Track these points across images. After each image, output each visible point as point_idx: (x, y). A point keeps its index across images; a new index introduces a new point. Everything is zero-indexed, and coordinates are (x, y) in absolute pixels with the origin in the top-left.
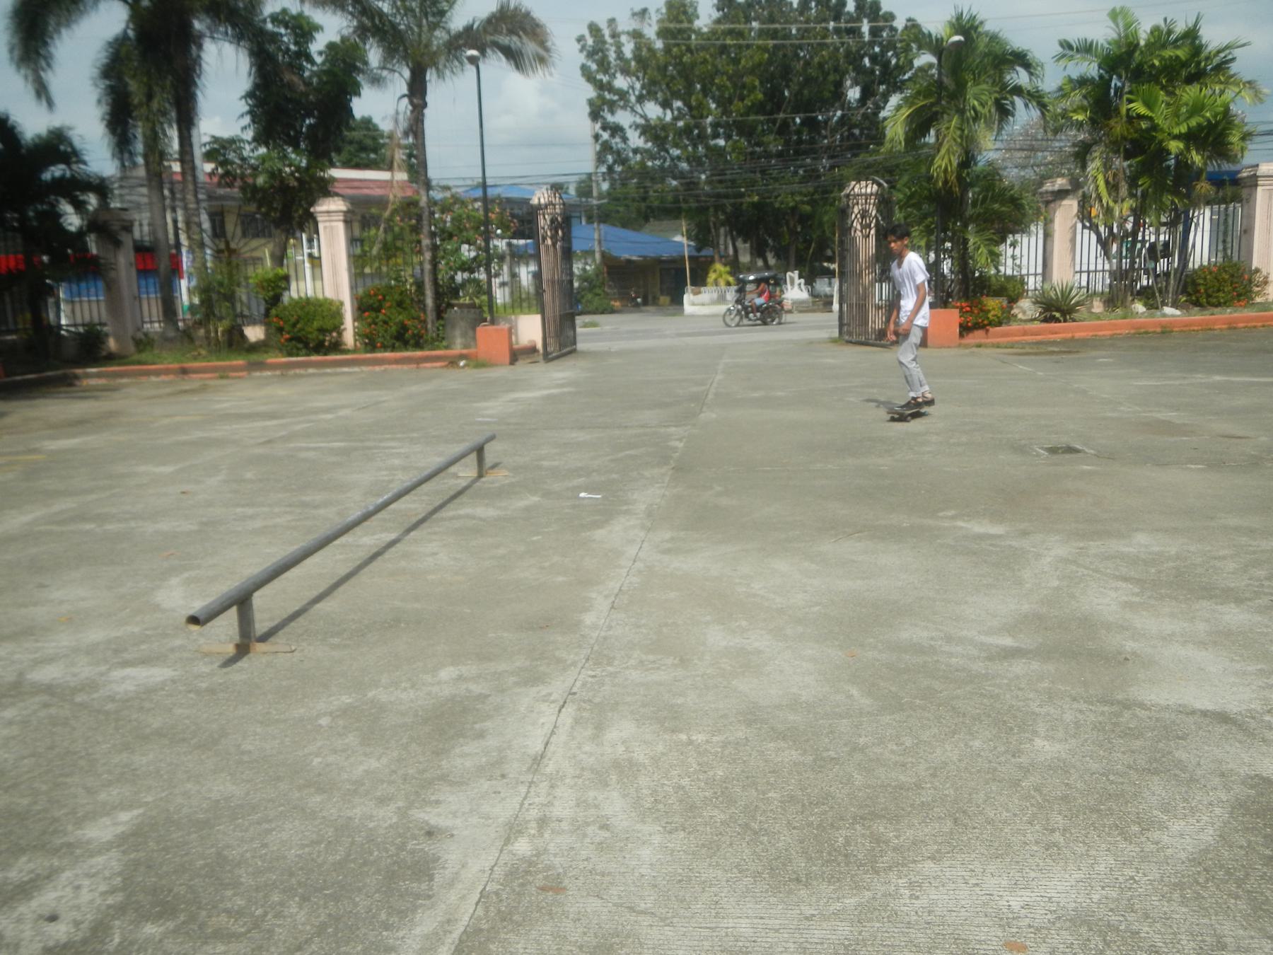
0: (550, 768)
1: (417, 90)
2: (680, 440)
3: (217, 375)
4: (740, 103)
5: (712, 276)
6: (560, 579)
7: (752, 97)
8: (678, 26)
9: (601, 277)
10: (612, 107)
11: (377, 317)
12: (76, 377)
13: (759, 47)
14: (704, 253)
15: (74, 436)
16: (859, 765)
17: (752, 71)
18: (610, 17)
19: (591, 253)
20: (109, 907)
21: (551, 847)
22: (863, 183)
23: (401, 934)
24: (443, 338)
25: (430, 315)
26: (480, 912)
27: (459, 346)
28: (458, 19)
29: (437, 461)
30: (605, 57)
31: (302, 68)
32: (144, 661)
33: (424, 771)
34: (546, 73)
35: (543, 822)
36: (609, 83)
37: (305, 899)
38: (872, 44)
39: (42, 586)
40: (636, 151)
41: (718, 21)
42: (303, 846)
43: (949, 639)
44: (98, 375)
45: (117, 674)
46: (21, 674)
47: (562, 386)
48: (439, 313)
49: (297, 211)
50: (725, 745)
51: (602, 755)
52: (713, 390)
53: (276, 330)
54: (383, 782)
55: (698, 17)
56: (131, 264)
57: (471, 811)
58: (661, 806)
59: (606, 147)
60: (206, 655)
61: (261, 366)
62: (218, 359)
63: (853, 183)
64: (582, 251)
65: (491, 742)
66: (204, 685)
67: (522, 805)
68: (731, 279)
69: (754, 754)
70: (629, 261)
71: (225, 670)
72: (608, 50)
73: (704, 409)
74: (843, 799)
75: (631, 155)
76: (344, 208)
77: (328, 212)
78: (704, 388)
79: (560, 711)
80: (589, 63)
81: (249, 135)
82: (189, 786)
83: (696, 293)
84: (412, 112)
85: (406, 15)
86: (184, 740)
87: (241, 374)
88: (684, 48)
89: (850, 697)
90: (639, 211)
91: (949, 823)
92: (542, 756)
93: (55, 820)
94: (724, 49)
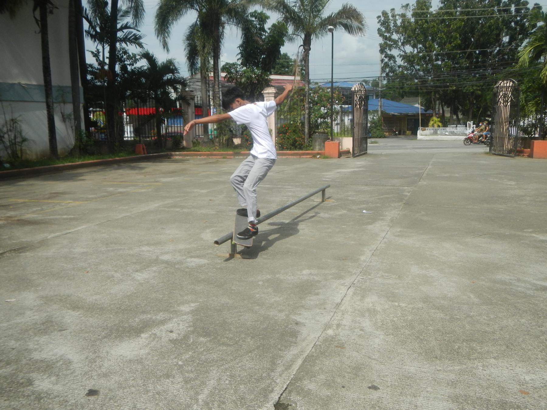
0: (343, 308)
1: (307, 43)
2: (409, 192)
3: (222, 157)
4: (450, 46)
5: (431, 123)
6: (352, 242)
7: (455, 42)
8: (422, 11)
11: (285, 136)
12: (172, 155)
13: (460, 20)
14: (429, 112)
15: (171, 177)
16: (469, 322)
17: (456, 30)
19: (376, 111)
20: (189, 331)
21: (341, 334)
22: (505, 82)
23: (285, 353)
24: (311, 146)
25: (306, 136)
26: (313, 350)
28: (326, 13)
29: (306, 194)
30: (389, 25)
31: (261, 35)
32: (198, 257)
33: (296, 303)
34: (362, 35)
35: (338, 325)
36: (390, 37)
37: (252, 337)
38: (516, 16)
39: (163, 228)
40: (399, 67)
41: (441, 8)
42: (252, 322)
43: (519, 280)
44: (179, 155)
45: (189, 260)
46: (157, 257)
47: (360, 167)
48: (310, 135)
49: (256, 92)
50: (413, 309)
51: (363, 306)
52: (426, 172)
54: (281, 305)
57: (312, 318)
58: (385, 326)
59: (386, 65)
60: (219, 257)
61: (238, 154)
62: (223, 151)
63: (501, 81)
65: (321, 297)
66: (219, 267)
67: (331, 319)
68: (440, 124)
69: (425, 313)
70: (393, 115)
71: (226, 262)
72: (390, 22)
73: (421, 180)
74: (460, 333)
75: (397, 68)
77: (268, 93)
79: (348, 289)
80: (382, 28)
81: (239, 62)
82: (214, 298)
83: (423, 130)
84: (304, 52)
85: (304, 12)
86: (212, 283)
88: (424, 21)
89: (470, 297)
90: (399, 93)
91: (504, 347)
92: (340, 304)
93: (171, 303)
94: (443, 21)
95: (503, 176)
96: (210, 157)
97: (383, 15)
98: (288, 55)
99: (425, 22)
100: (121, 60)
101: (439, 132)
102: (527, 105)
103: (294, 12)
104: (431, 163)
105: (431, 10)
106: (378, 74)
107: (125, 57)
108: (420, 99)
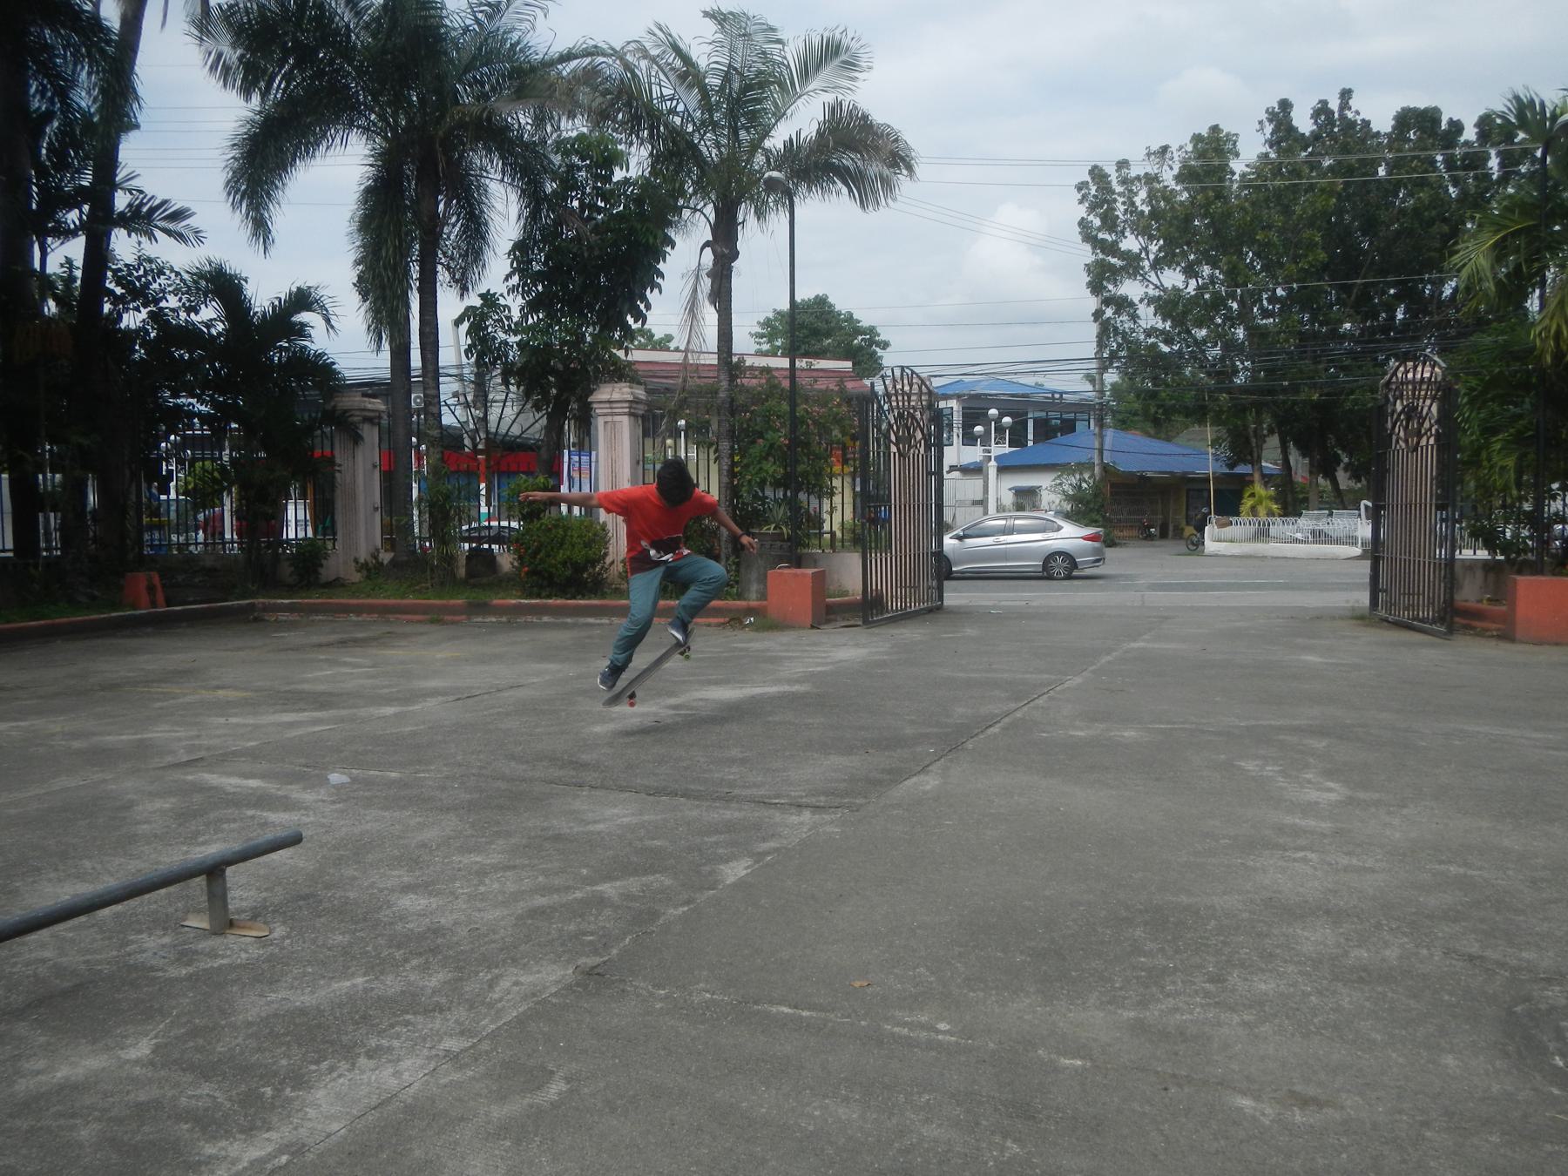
4: (1293, 266)
5: (1248, 503)
10: (1114, 274)
14: (1241, 469)
17: (1311, 224)
18: (1120, 158)
19: (1091, 466)
22: (1410, 364)
24: (737, 582)
27: (753, 595)
28: (776, 141)
36: (1115, 243)
40: (1149, 333)
44: (291, 609)
52: (1019, 715)
53: (520, 558)
55: (1237, 155)
56: (375, 466)
59: (1106, 330)
61: (482, 608)
62: (440, 598)
70: (1143, 479)
76: (631, 398)
78: (1013, 705)
87: (457, 618)
88: (1211, 194)
94: (1278, 194)
95: (1320, 744)
96: (391, 617)
97: (1093, 179)
98: (831, 300)
100: (138, 293)
101: (1273, 530)
102: (1487, 445)
104: (1105, 659)
105: (1238, 166)
106: (1090, 350)
107: (155, 286)
108: (1209, 432)
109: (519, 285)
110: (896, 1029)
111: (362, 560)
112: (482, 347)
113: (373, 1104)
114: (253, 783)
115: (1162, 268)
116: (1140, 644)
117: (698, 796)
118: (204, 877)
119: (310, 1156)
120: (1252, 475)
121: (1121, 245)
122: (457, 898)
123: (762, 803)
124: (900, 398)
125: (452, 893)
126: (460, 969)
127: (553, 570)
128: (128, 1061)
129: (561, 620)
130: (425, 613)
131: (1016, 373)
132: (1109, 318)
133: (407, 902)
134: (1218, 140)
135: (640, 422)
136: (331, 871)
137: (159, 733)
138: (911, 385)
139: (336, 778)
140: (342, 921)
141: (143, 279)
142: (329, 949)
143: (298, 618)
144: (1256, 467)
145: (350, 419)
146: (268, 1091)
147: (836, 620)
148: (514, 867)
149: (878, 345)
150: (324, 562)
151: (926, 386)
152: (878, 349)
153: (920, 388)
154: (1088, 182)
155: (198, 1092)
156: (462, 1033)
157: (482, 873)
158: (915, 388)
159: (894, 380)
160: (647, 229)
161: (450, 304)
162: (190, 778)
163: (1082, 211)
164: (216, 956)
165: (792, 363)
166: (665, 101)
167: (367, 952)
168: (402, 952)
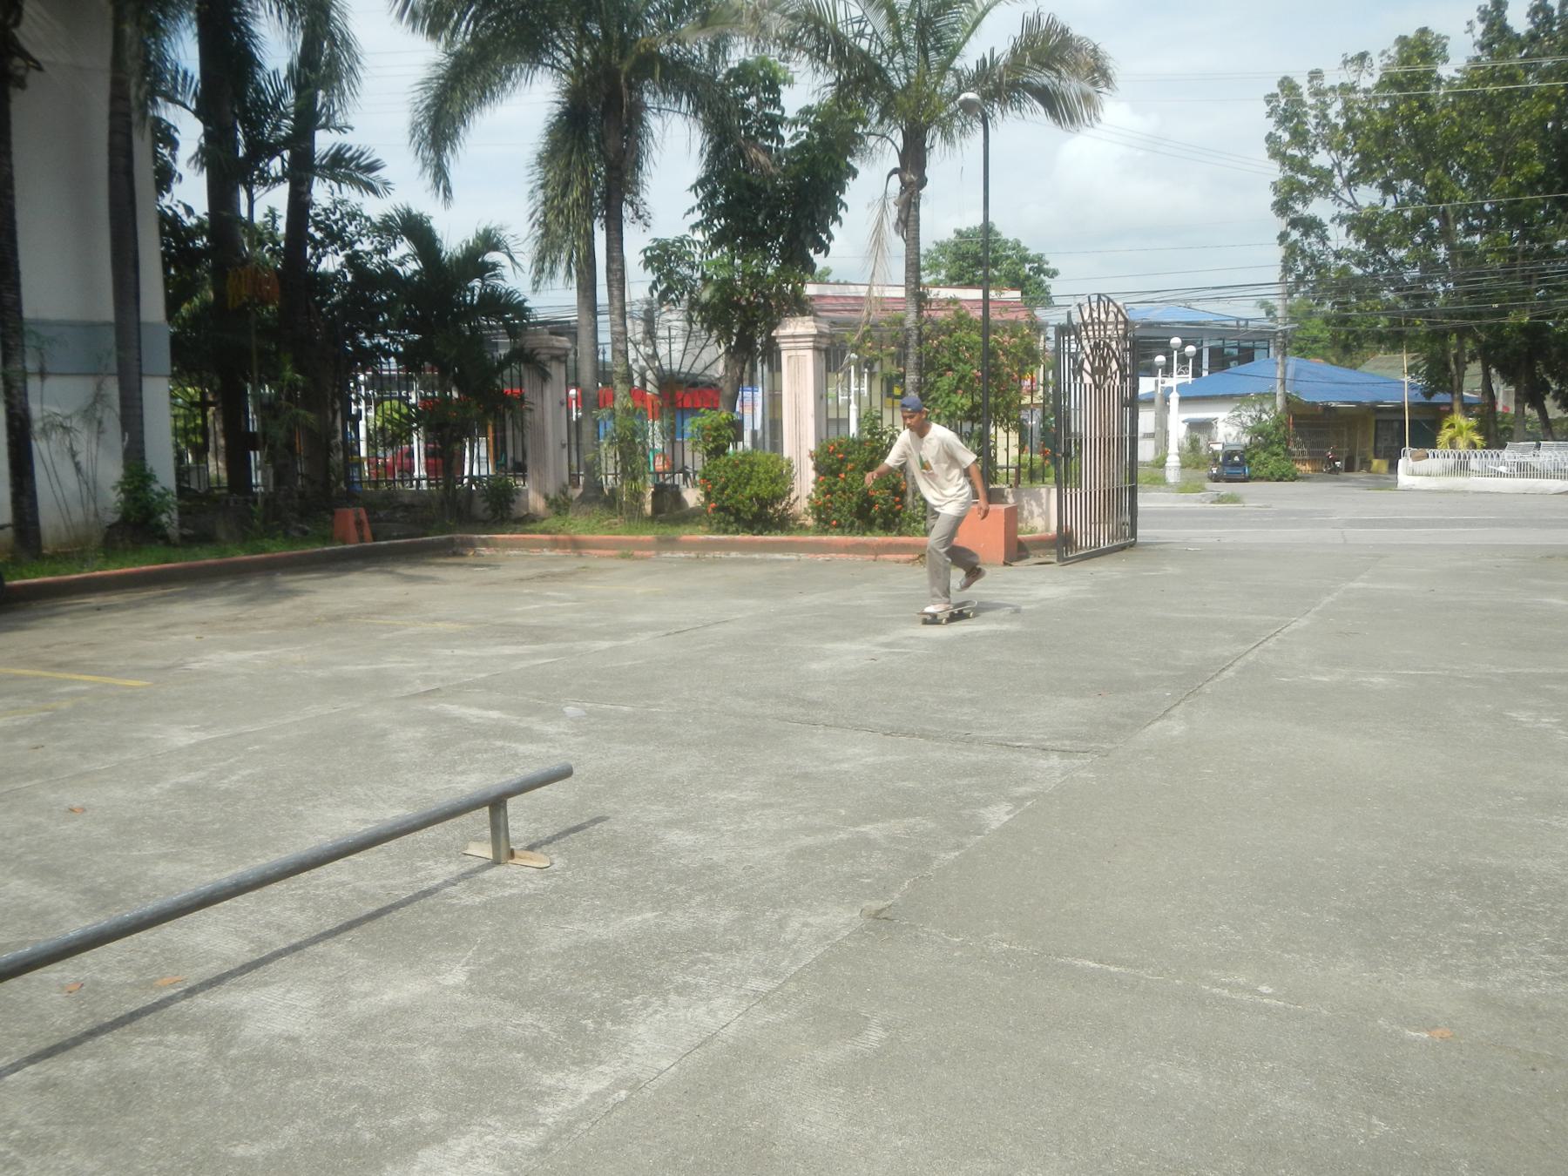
1: (913, 161)
4: (1505, 179)
5: (1445, 435)
7: (1525, 170)
9: (1282, 430)
10: (1305, 193)
11: (835, 484)
14: (1440, 398)
18: (1313, 68)
28: (968, 60)
36: (1306, 158)
40: (1338, 255)
44: (485, 543)
52: (1251, 657)
53: (707, 495)
55: (1446, 60)
61: (671, 544)
62: (630, 533)
64: (1259, 394)
68: (1477, 438)
70: (1327, 409)
75: (1332, 259)
76: (815, 332)
77: (794, 336)
78: (1242, 648)
87: (647, 553)
88: (1415, 104)
94: (1489, 101)
97: (1282, 91)
99: (1421, 107)
100: (335, 237)
101: (1474, 464)
103: (865, 56)
105: (1445, 71)
106: (1275, 274)
107: (351, 229)
108: (1405, 359)
109: (702, 221)
110: (1215, 990)
111: (552, 496)
112: (670, 284)
113: (697, 1041)
114: (494, 714)
115: (1356, 185)
116: (1361, 585)
117: (936, 738)
118: (487, 809)
119: (648, 1093)
120: (1451, 405)
121: (1311, 161)
122: (723, 835)
123: (1003, 745)
124: (1096, 327)
125: (717, 830)
126: (746, 907)
127: (741, 507)
128: (447, 987)
129: (748, 556)
130: (614, 549)
131: (1198, 300)
132: (1296, 241)
133: (675, 837)
134: (1425, 44)
135: (823, 356)
136: (593, 804)
137: (391, 663)
138: (1107, 314)
139: (569, 710)
140: (615, 854)
141: (340, 223)
142: (611, 882)
143: (494, 553)
144: (1456, 396)
145: (538, 358)
146: (590, 1024)
147: (1027, 557)
148: (771, 805)
149: (1046, 273)
150: (515, 497)
151: (1123, 315)
152: (1046, 278)
153: (1116, 316)
154: (1277, 95)
155: (522, 1021)
156: (765, 973)
157: (741, 810)
158: (1112, 317)
159: (1091, 309)
160: (830, 158)
161: (635, 242)
162: (432, 708)
163: (1270, 125)
164: (505, 885)
165: (986, 295)
166: (852, 23)
167: (649, 886)
168: (683, 888)
